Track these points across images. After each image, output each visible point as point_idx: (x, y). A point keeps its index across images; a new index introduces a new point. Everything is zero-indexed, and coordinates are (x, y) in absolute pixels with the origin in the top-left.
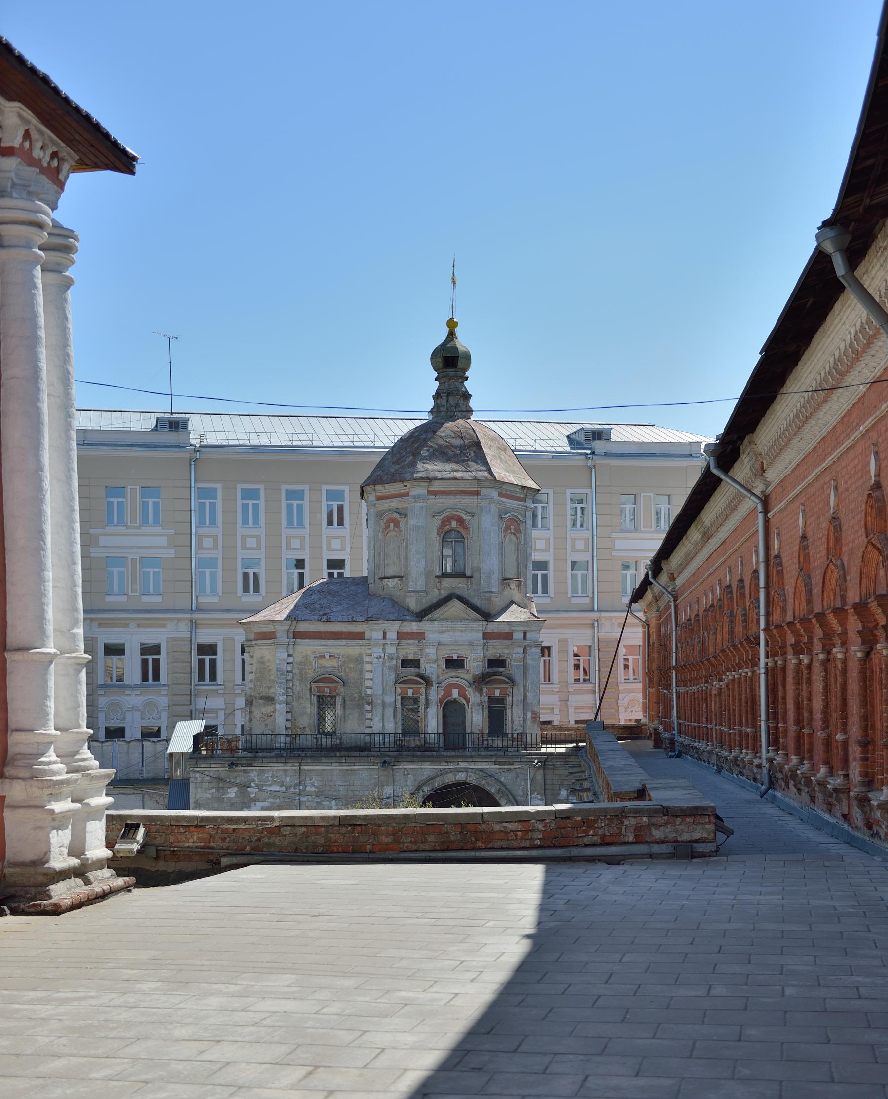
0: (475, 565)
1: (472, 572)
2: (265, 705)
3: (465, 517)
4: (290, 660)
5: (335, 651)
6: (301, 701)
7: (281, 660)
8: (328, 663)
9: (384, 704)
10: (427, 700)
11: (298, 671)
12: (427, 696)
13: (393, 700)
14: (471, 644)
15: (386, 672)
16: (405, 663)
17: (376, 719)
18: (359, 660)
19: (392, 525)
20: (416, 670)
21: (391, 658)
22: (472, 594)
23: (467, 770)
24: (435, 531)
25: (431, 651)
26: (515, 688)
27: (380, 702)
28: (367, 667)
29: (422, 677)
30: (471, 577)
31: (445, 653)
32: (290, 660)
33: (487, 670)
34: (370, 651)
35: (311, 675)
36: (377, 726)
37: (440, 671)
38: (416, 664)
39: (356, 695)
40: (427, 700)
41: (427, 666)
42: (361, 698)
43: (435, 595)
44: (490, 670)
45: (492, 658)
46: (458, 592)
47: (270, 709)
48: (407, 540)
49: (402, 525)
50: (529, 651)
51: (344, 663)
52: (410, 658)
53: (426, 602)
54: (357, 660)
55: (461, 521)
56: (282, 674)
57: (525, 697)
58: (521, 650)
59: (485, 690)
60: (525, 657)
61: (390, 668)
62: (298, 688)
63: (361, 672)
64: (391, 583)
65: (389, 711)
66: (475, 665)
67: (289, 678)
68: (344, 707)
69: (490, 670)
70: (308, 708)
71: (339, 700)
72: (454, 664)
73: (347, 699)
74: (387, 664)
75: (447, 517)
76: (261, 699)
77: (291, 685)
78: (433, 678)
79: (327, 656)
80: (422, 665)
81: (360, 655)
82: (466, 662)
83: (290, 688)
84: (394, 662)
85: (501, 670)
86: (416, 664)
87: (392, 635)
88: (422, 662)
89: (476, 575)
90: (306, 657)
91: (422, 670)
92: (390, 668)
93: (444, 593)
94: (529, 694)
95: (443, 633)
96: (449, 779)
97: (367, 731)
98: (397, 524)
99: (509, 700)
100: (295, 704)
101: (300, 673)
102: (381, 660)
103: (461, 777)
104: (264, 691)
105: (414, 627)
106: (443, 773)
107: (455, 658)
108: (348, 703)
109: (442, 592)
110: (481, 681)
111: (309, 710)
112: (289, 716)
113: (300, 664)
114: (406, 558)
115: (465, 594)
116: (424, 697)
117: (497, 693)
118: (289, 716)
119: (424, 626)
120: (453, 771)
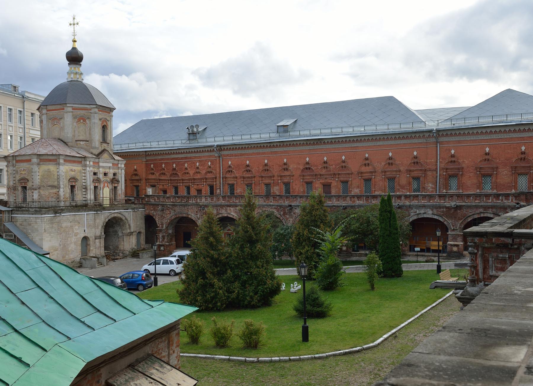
2: (51, 189)
18: (80, 172)
19: (82, 121)
23: (117, 213)
35: (69, 178)
47: (55, 190)
48: (90, 127)
49: (87, 121)
64: (81, 143)
65: (92, 191)
66: (111, 176)
70: (68, 190)
71: (76, 187)
72: (105, 174)
76: (49, 186)
82: (109, 174)
87: (92, 163)
90: (67, 170)
93: (103, 148)
96: (113, 216)
97: (84, 199)
98: (84, 120)
103: (116, 215)
104: (50, 183)
114: (90, 134)
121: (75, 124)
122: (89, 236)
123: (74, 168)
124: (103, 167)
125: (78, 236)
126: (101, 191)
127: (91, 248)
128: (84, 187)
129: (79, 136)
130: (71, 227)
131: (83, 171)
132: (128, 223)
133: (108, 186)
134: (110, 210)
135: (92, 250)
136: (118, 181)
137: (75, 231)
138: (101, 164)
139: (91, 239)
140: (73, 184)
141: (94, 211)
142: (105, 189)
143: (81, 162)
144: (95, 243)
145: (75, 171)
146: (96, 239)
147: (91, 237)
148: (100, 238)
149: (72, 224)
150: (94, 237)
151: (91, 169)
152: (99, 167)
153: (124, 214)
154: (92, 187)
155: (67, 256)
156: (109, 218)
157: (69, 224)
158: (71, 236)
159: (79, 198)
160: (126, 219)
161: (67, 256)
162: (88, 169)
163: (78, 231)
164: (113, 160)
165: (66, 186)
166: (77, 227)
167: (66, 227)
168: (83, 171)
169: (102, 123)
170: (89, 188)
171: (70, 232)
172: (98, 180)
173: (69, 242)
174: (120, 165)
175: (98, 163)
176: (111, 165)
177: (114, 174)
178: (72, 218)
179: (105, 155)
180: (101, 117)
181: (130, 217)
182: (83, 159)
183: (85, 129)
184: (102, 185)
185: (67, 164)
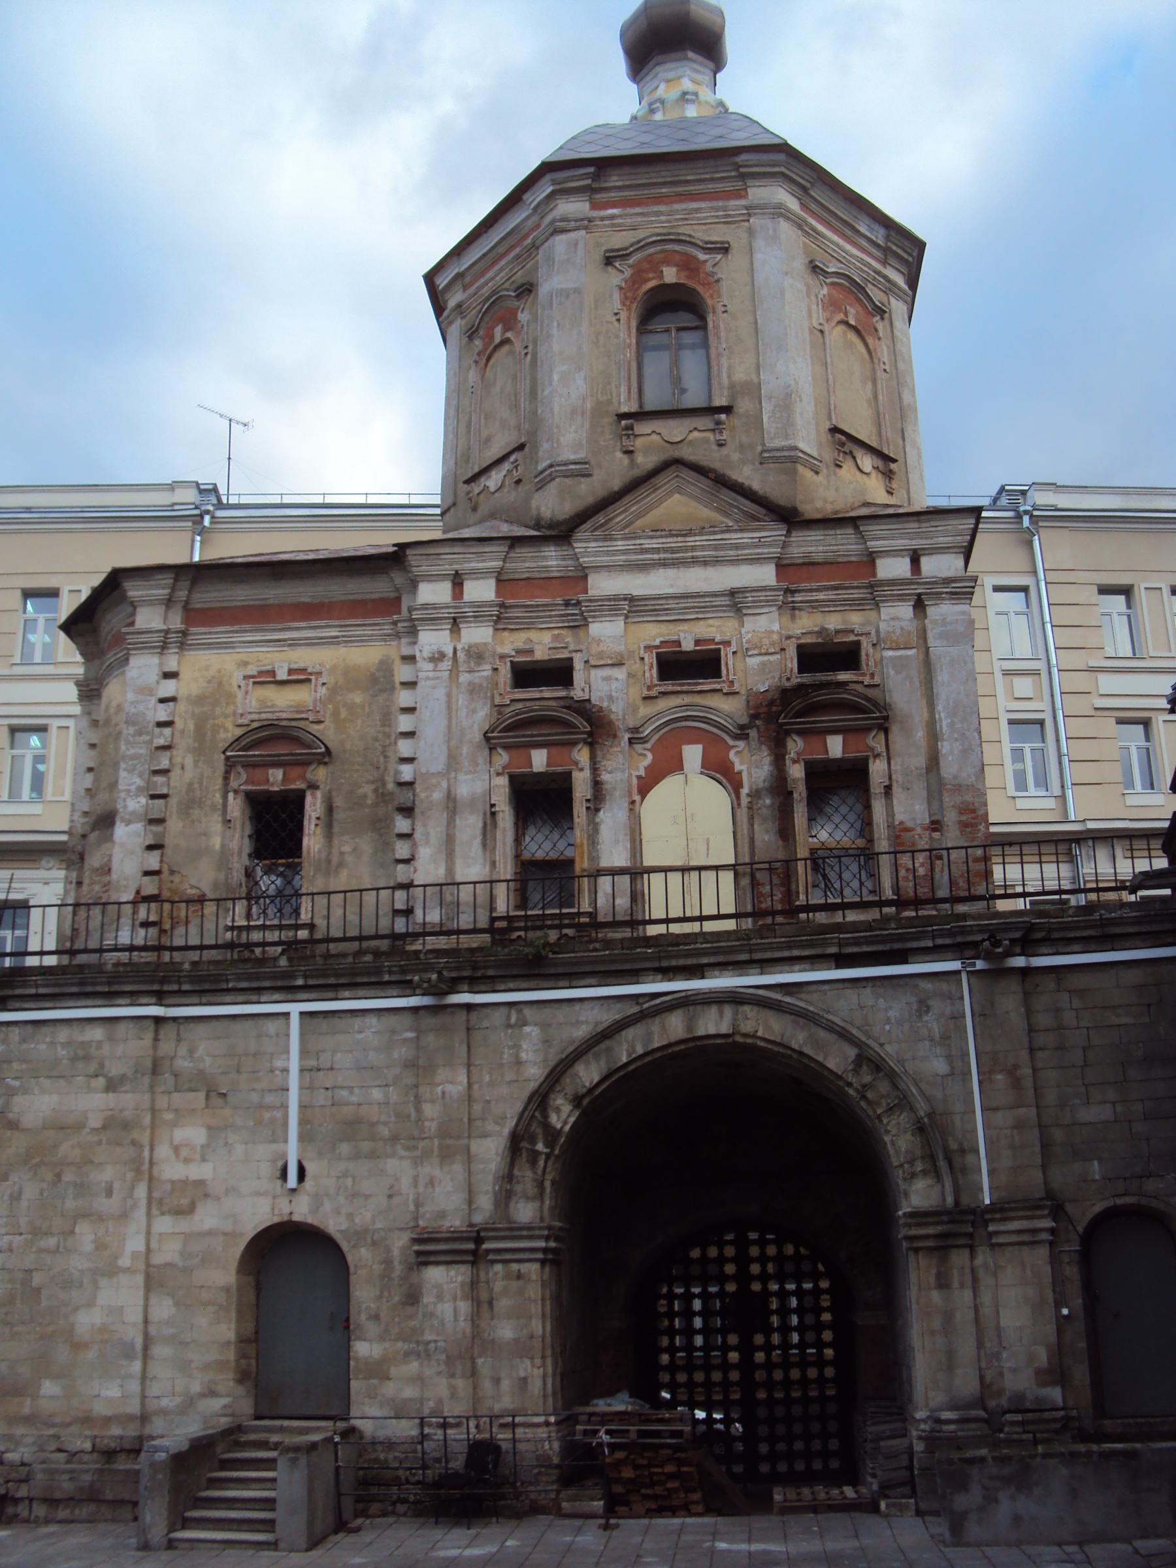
0: (740, 376)
1: (733, 396)
3: (702, 256)
4: (168, 688)
5: (304, 657)
6: (196, 813)
7: (148, 690)
8: (284, 701)
9: (452, 805)
10: (597, 784)
11: (191, 725)
12: (595, 770)
13: (480, 787)
14: (736, 601)
15: (462, 700)
16: (527, 674)
17: (424, 853)
18: (380, 681)
20: (562, 693)
21: (476, 654)
22: (735, 456)
23: (734, 998)
24: (617, 296)
25: (607, 632)
26: (895, 731)
27: (438, 795)
28: (404, 698)
29: (583, 709)
30: (727, 410)
31: (653, 633)
32: (168, 688)
33: (796, 680)
34: (406, 651)
36: (428, 868)
37: (636, 693)
38: (558, 673)
39: (367, 790)
40: (597, 784)
41: (596, 674)
42: (383, 796)
43: (613, 470)
44: (807, 678)
45: (809, 640)
46: (687, 453)
49: (523, 317)
50: (931, 611)
51: (334, 691)
52: (541, 654)
53: (587, 491)
54: (374, 679)
55: (689, 266)
56: (140, 733)
57: (934, 761)
58: (905, 610)
59: (795, 745)
60: (923, 634)
61: (473, 690)
62: (189, 774)
63: (387, 719)
64: (493, 480)
65: (470, 825)
67: (161, 742)
68: (329, 826)
69: (807, 678)
70: (218, 840)
71: (313, 807)
73: (338, 802)
74: (464, 678)
75: (649, 259)
77: (164, 763)
78: (617, 710)
79: (282, 675)
80: (578, 676)
81: (385, 667)
82: (728, 660)
83: (165, 772)
84: (486, 671)
85: (843, 676)
86: (558, 673)
87: (481, 591)
88: (578, 665)
89: (744, 406)
91: (577, 693)
92: (473, 690)
93: (646, 461)
94: (945, 747)
95: (643, 567)
96: (675, 1026)
99: (877, 769)
100: (175, 825)
101: (199, 728)
102: (446, 665)
103: (713, 1023)
105: (552, 559)
106: (651, 1010)
107: (688, 645)
108: (339, 815)
109: (640, 459)
110: (778, 716)
111: (216, 842)
112: (153, 861)
113: (200, 700)
114: (533, 393)
115: (711, 457)
116: (587, 773)
117: (835, 746)
118: (153, 861)
119: (586, 547)
120: (685, 1002)
121: (473, 376)
122: (334, 1225)
123: (282, 661)
124: (634, 607)
125: (207, 1218)
126: (612, 819)
127: (362, 1349)
128: (404, 797)
129: (488, 440)
130: (117, 1125)
131: (403, 673)
132: (903, 1102)
133: (719, 769)
134: (634, 975)
135: (378, 1371)
136: (872, 715)
137: (171, 1170)
138: (602, 585)
139: (360, 1258)
140: (276, 778)
141: (407, 987)
142: (667, 789)
143: (390, 606)
144: (413, 1298)
145: (300, 678)
146: (424, 1259)
147: (360, 1236)
148: (471, 1248)
149: (128, 1101)
150: (400, 1243)
151: (478, 634)
152: (578, 611)
153: (843, 1008)
154: (485, 783)
155: (49, 1388)
156: (629, 1047)
157: (93, 1103)
158: (111, 1205)
159: (341, 878)
160: (867, 1060)
161: (49, 1388)
162: (432, 639)
163: (196, 1172)
164: (774, 532)
165: (190, 804)
166: (193, 1134)
167: (64, 1127)
168: (403, 673)
169: (637, 278)
170: (431, 796)
171: (107, 1174)
172: (594, 726)
173: (77, 1264)
174: (893, 568)
175: (580, 577)
176: (766, 575)
177: (828, 657)
178: (137, 1046)
179: (677, 504)
180: (620, 240)
181: (950, 1038)
182: (399, 579)
183: (515, 378)
184: (621, 767)
185: (220, 633)
